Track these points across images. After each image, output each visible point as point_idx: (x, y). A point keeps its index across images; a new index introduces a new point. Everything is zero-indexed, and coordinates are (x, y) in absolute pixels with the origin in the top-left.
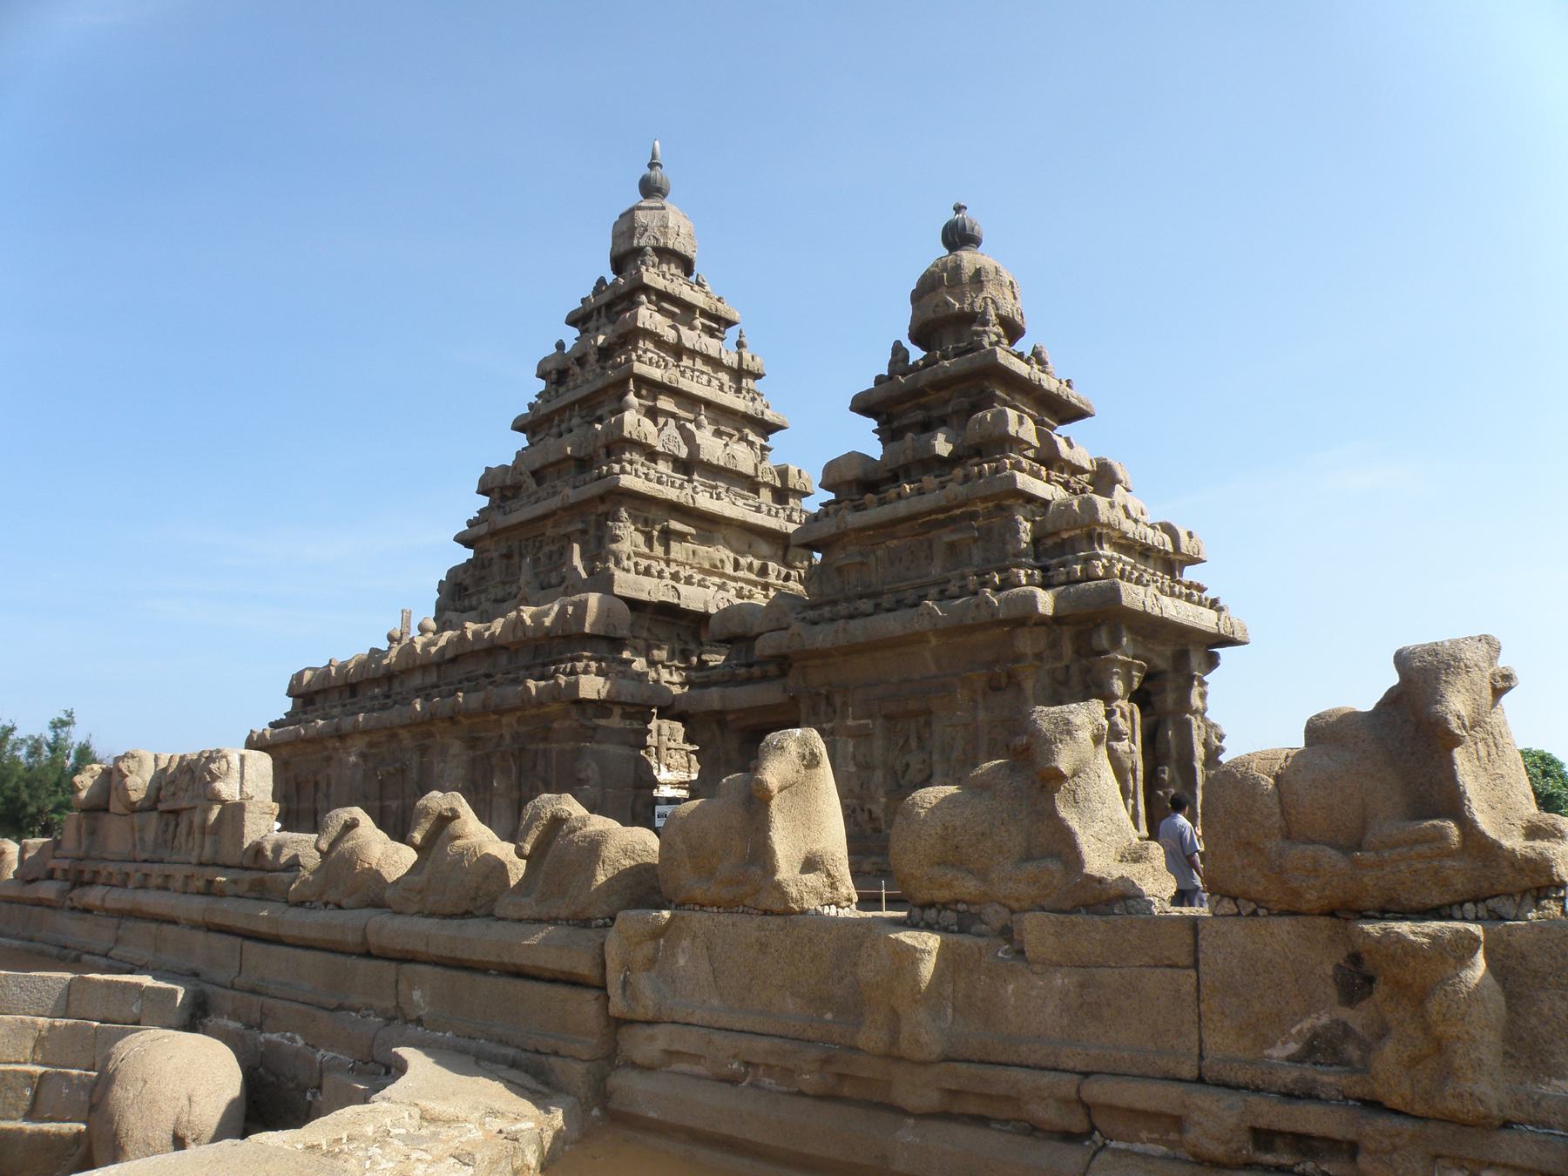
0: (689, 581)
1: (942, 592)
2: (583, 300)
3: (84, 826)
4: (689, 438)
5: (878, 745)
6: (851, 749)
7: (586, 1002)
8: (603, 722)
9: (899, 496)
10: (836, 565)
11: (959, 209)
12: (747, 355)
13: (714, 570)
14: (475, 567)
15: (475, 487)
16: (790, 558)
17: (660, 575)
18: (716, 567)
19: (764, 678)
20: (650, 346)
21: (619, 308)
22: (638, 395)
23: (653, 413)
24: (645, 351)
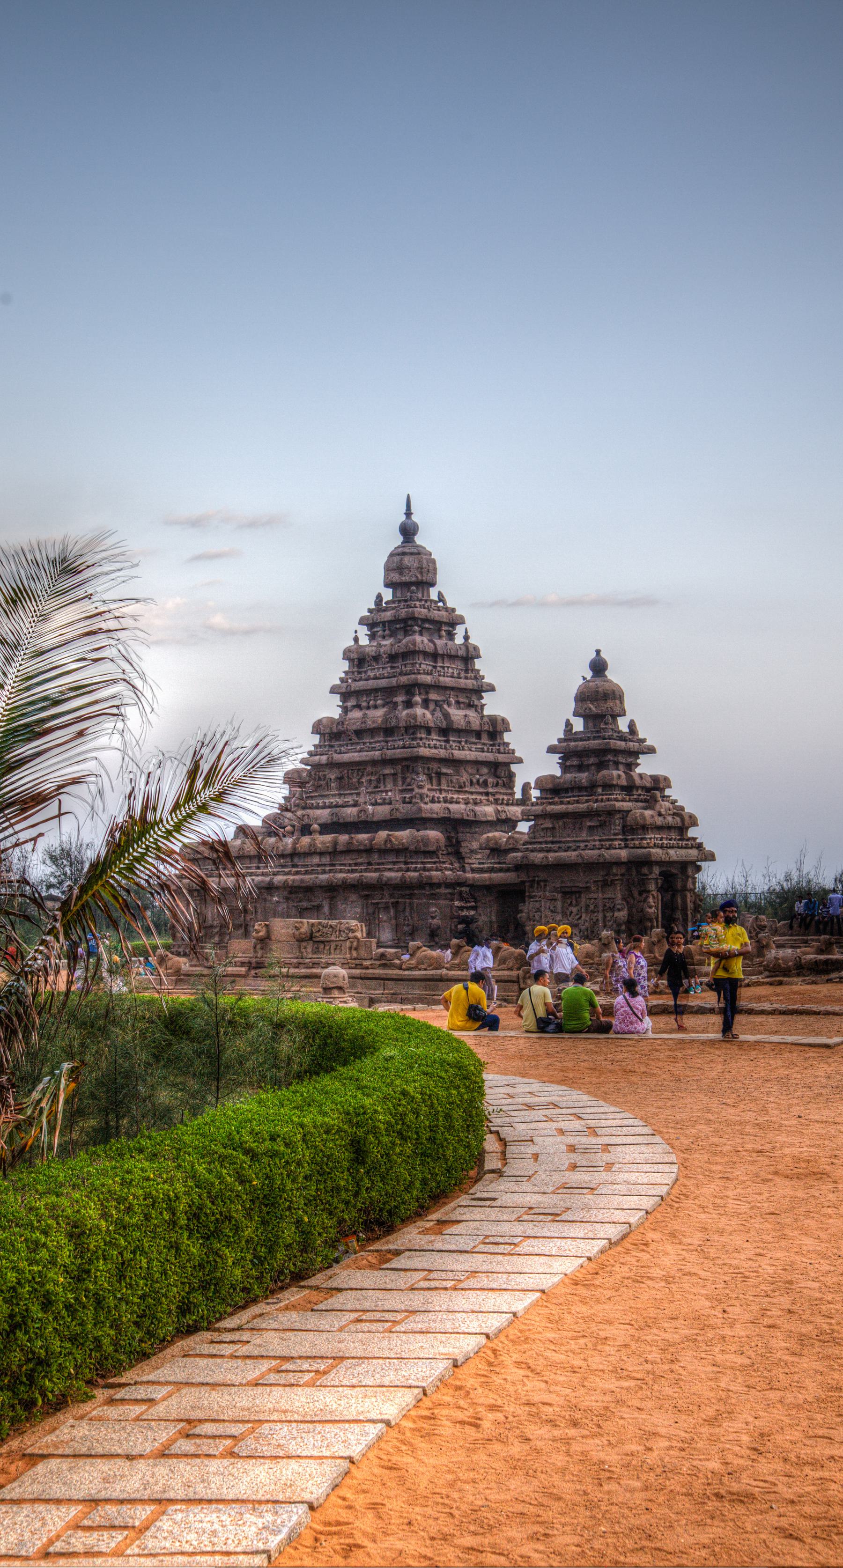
0: (451, 802)
1: (586, 846)
2: (370, 611)
3: (259, 946)
4: (446, 716)
5: (559, 904)
7: (515, 987)
8: (438, 891)
9: (569, 803)
11: (598, 652)
12: (471, 649)
13: (461, 789)
14: (315, 779)
15: (311, 729)
16: (498, 773)
17: (439, 802)
18: (460, 787)
19: (507, 870)
20: (421, 660)
21: (398, 626)
23: (426, 703)
24: (420, 664)
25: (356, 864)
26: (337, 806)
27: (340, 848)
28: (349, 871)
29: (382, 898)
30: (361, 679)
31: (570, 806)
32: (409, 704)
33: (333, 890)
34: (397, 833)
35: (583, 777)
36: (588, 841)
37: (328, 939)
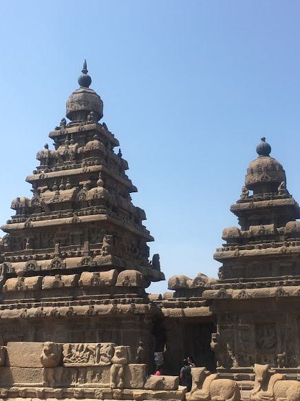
1: (280, 283)
6: (240, 334)
9: (260, 248)
10: (233, 268)
11: (263, 139)
19: (199, 305)
21: (81, 136)
22: (102, 179)
25: (61, 300)
26: (31, 258)
27: (44, 286)
28: (55, 305)
29: (88, 328)
30: (51, 171)
31: (263, 250)
32: (90, 187)
33: (39, 320)
34: (101, 273)
35: (270, 227)
36: (282, 279)
37: (84, 364)
